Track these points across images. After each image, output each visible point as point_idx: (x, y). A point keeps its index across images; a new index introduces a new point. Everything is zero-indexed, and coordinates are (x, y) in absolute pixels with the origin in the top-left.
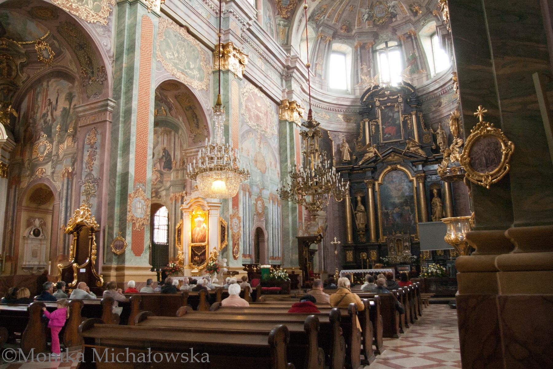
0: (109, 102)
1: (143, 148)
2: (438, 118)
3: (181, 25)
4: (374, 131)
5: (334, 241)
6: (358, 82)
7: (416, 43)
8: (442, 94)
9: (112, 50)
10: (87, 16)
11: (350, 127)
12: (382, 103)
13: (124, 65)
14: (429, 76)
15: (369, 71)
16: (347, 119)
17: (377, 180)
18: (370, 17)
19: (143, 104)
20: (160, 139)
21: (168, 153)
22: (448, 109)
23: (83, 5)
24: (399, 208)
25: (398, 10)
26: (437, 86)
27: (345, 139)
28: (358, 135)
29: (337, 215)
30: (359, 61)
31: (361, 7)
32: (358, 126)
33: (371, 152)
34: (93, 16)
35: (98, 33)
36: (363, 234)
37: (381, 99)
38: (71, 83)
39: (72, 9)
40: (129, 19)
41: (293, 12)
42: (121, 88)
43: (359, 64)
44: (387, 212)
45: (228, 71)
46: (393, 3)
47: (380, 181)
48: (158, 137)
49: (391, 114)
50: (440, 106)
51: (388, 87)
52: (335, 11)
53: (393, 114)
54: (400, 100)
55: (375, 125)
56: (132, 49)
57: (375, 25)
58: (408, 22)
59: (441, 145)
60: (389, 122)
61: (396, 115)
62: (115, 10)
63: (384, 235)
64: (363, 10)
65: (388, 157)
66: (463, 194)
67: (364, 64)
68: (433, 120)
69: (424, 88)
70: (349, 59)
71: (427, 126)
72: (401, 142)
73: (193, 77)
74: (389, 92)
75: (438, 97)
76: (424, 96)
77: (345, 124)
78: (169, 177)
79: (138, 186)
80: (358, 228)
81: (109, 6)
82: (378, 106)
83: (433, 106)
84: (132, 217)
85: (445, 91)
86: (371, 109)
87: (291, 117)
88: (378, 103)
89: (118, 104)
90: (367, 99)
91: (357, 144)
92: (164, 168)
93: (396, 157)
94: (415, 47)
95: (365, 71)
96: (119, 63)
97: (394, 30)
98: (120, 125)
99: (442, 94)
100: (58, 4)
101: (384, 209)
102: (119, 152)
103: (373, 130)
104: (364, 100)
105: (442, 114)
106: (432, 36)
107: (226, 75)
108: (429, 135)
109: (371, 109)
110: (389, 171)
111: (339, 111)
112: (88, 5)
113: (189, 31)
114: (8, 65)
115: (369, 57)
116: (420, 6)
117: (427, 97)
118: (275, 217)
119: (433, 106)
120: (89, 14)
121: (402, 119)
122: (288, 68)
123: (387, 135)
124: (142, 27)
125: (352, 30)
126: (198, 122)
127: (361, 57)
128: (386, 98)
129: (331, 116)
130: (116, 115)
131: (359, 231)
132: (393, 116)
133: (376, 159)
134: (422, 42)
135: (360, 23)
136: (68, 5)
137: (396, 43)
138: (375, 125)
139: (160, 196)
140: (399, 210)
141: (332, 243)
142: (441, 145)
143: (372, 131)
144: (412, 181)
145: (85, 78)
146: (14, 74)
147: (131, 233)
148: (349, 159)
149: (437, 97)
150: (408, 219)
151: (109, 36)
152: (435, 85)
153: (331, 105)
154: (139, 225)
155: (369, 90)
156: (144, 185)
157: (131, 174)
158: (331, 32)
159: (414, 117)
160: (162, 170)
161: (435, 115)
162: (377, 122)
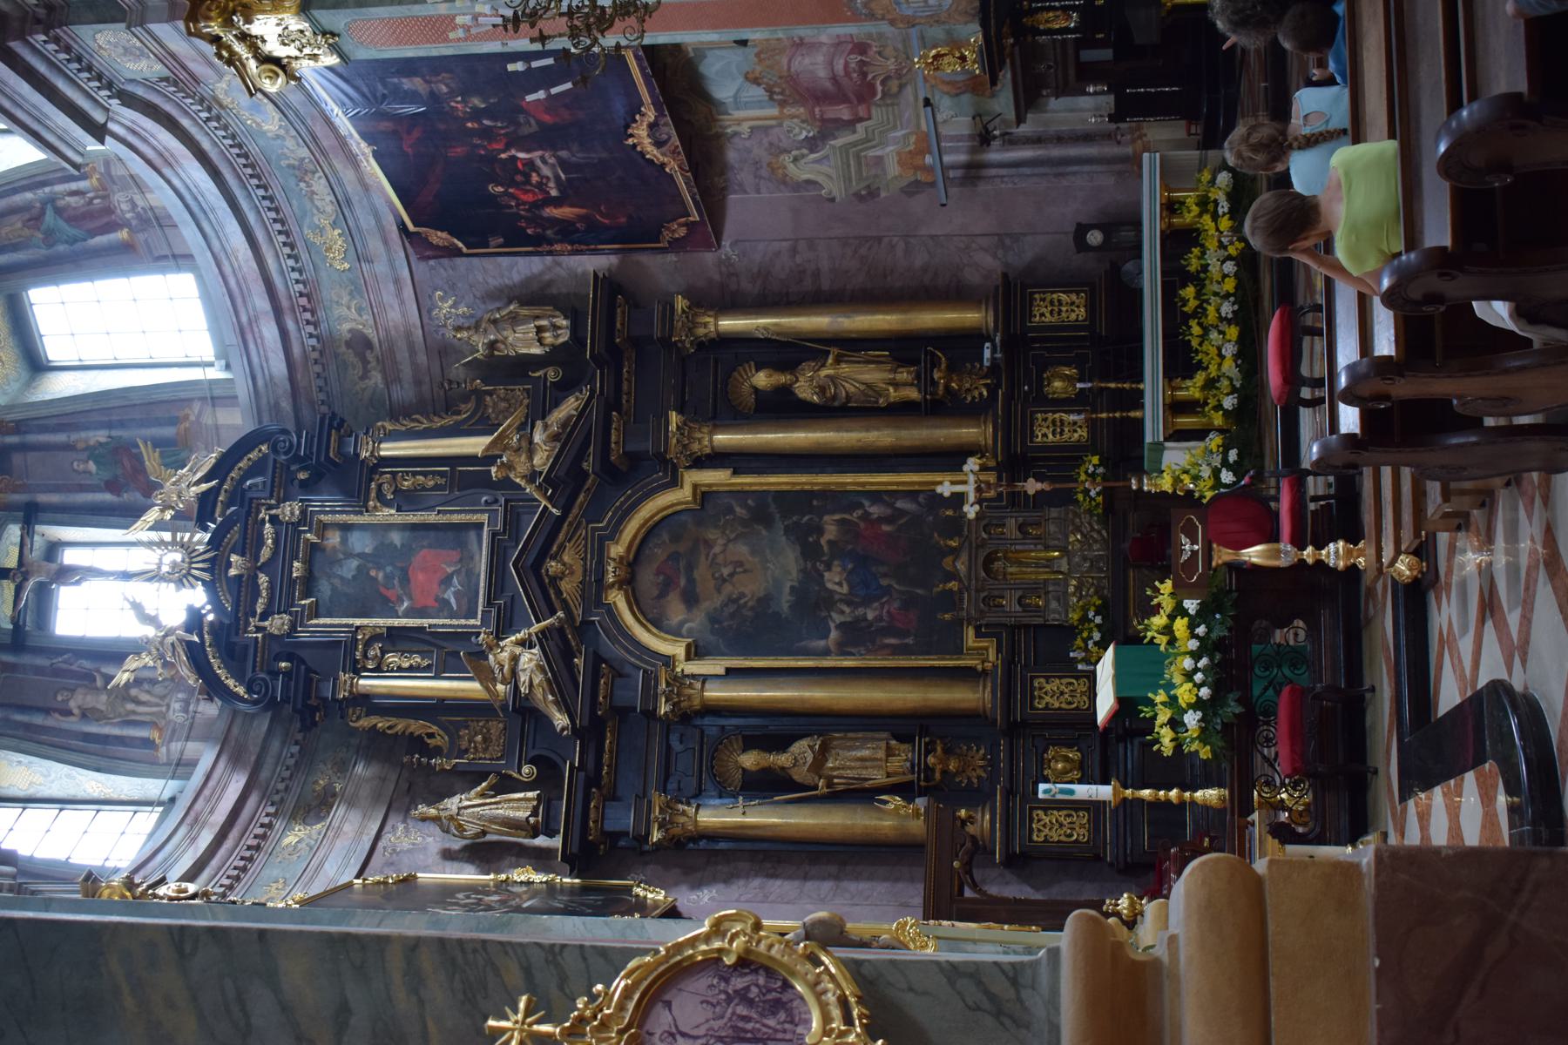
2: (422, 358)
4: (417, 659)
5: (959, 499)
6: (148, 743)
7: (45, 429)
8: (316, 325)
11: (365, 791)
12: (280, 602)
14: (217, 393)
17: (668, 661)
24: (829, 568)
26: (270, 331)
27: (422, 809)
28: (417, 744)
29: (827, 886)
30: (38, 720)
32: (377, 746)
33: (515, 659)
36: (948, 752)
37: (259, 611)
43: (52, 721)
44: (840, 626)
47: (677, 649)
49: (350, 568)
50: (368, 344)
51: (212, 561)
53: (349, 555)
54: (290, 510)
55: (383, 652)
59: (548, 337)
60: (387, 577)
61: (362, 543)
63: (958, 651)
65: (559, 592)
66: (794, 251)
67: (66, 701)
68: (426, 388)
69: (264, 401)
71: (449, 407)
72: (499, 527)
74: (234, 558)
75: (326, 346)
76: (306, 413)
77: (339, 812)
80: (909, 777)
82: (293, 627)
83: (362, 385)
85: (303, 301)
88: (278, 624)
90: (240, 679)
91: (462, 753)
93: (566, 558)
94: (61, 438)
99: (316, 325)
101: (822, 643)
103: (406, 665)
104: (241, 690)
105: (408, 335)
106: (36, 365)
108: (490, 393)
110: (635, 602)
111: (264, 837)
115: (39, 671)
117: (312, 403)
119: (362, 385)
121: (388, 514)
123: (449, 595)
127: (23, 708)
128: (263, 579)
129: (275, 872)
131: (929, 770)
132: (361, 556)
133: (557, 647)
134: (48, 397)
138: (383, 652)
140: (836, 567)
141: (971, 511)
142: (548, 337)
143: (411, 669)
144: (705, 496)
148: (530, 794)
149: (321, 353)
150: (886, 528)
152: (260, 340)
153: (215, 862)
155: (196, 655)
161: (407, 372)
162: (375, 638)
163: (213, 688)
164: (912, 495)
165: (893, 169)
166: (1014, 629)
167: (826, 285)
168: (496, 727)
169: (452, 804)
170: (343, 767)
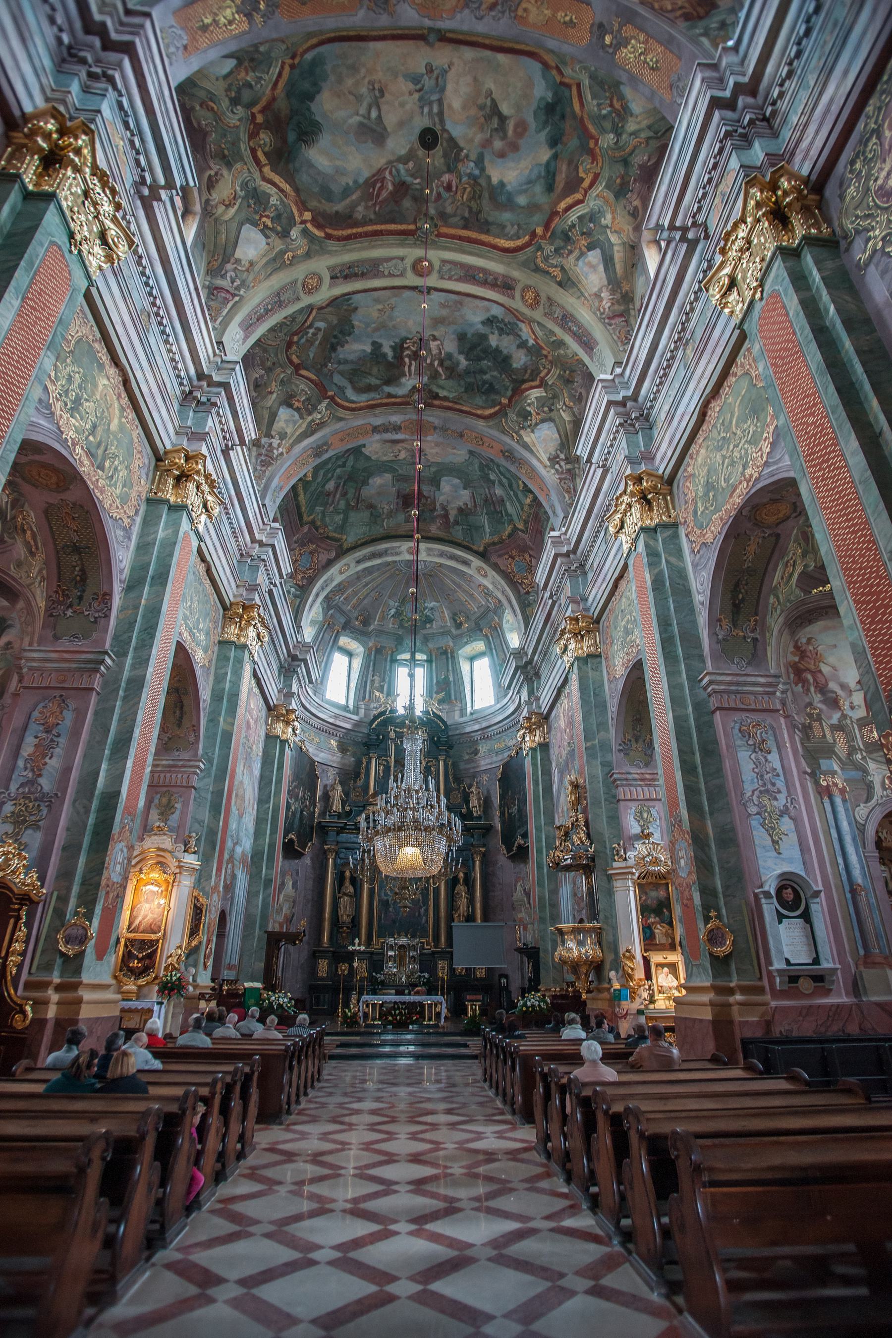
3: (203, 560)
6: (364, 698)
11: (346, 761)
13: (143, 602)
15: (382, 687)
16: (342, 748)
18: (398, 614)
22: (488, 761)
23: (110, 486)
25: (437, 614)
26: (477, 727)
28: (357, 775)
29: (310, 897)
31: (390, 597)
32: (359, 763)
38: (7, 600)
39: (97, 487)
40: (165, 529)
41: (311, 581)
42: (131, 638)
43: (371, 672)
45: (245, 646)
46: (433, 604)
52: (355, 593)
56: (162, 578)
57: (401, 626)
58: (446, 633)
62: (143, 508)
63: (379, 936)
64: (391, 603)
70: (357, 663)
73: (198, 644)
75: (476, 743)
77: (340, 755)
86: (382, 741)
87: (283, 732)
88: (392, 735)
89: (121, 666)
95: (377, 684)
96: (132, 595)
97: (426, 639)
98: (118, 703)
102: (107, 752)
106: (472, 659)
107: (239, 651)
109: (382, 741)
113: (208, 571)
116: (468, 618)
118: (242, 893)
122: (294, 658)
125: (370, 625)
126: (181, 717)
130: (112, 684)
135: (383, 618)
137: (425, 657)
145: (61, 603)
158: (343, 620)
159: (441, 763)
161: (468, 766)
163: (376, 717)
164: (427, 921)
165: (520, 916)
166: (383, 954)
167: (491, 894)
168: (361, 799)
169: (339, 788)
170: (354, 754)
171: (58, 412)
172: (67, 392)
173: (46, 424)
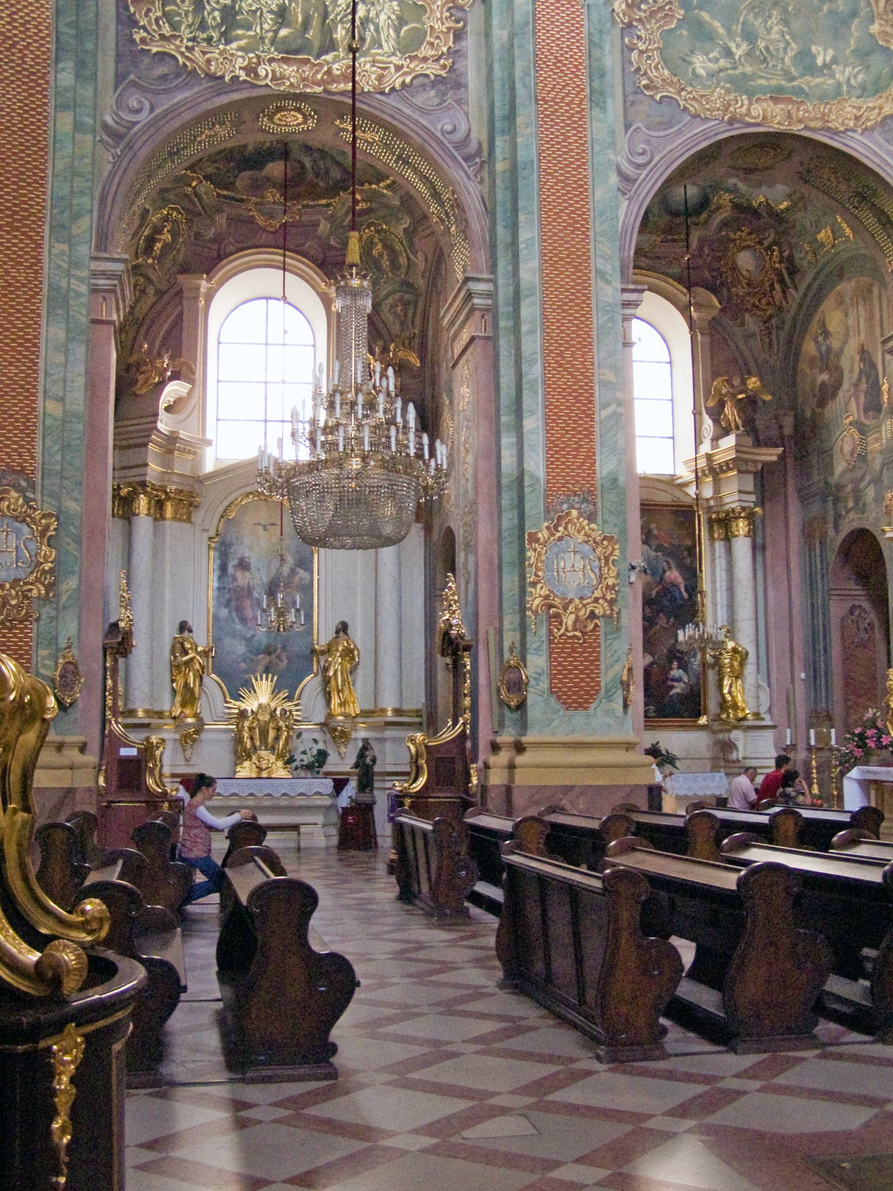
0: (471, 285)
1: (575, 391)
9: (474, 135)
10: (380, 78)
19: (562, 259)
20: (851, 322)
21: (870, 360)
34: (398, 68)
35: (421, 110)
39: (334, 79)
48: (846, 315)
78: (877, 440)
79: (565, 506)
81: (451, 15)
84: (546, 597)
92: (866, 412)
100: (292, 84)
112: (380, 46)
114: (385, 246)
120: (386, 68)
124: (534, 33)
136: (319, 76)
139: (865, 505)
146: (403, 260)
147: (545, 646)
151: (459, 102)
154: (577, 619)
156: (585, 500)
157: (532, 476)
160: (863, 419)
171: (201, 60)
172: (203, 26)
173: (188, 94)
